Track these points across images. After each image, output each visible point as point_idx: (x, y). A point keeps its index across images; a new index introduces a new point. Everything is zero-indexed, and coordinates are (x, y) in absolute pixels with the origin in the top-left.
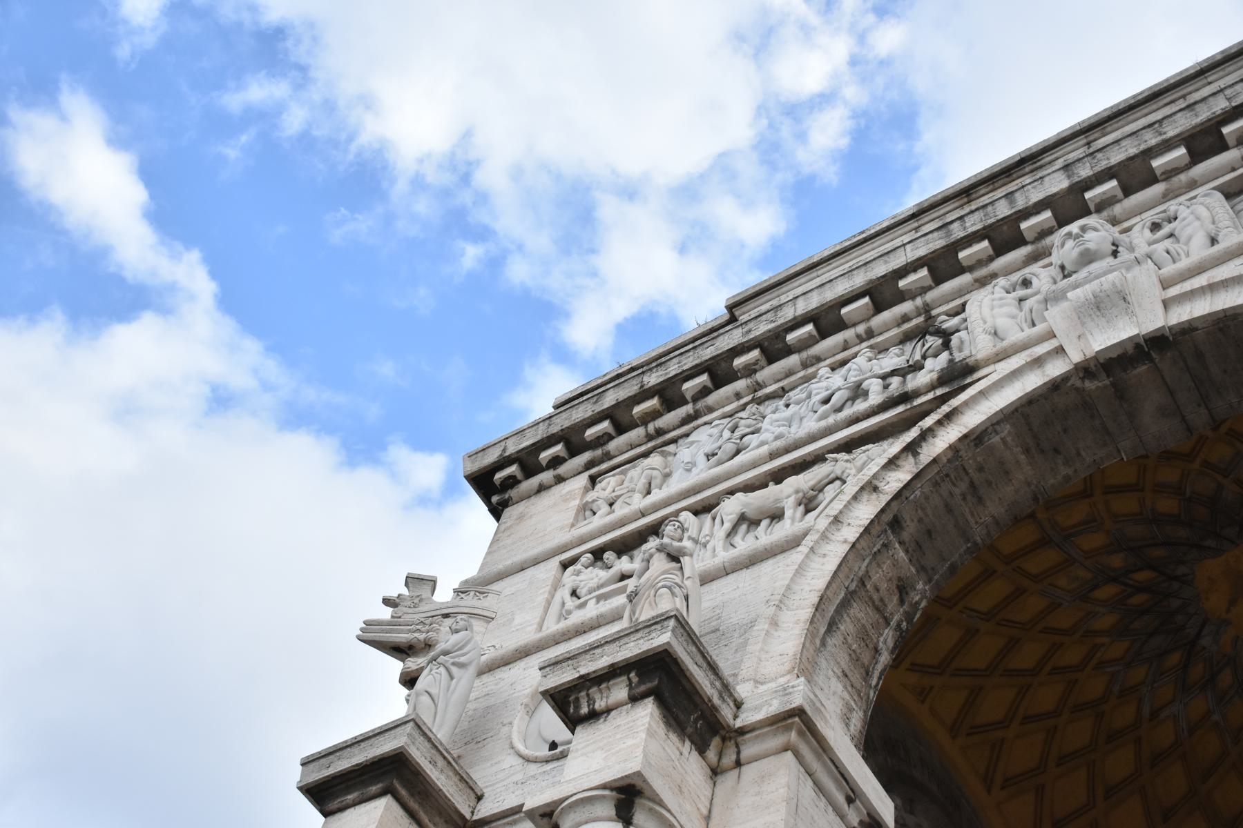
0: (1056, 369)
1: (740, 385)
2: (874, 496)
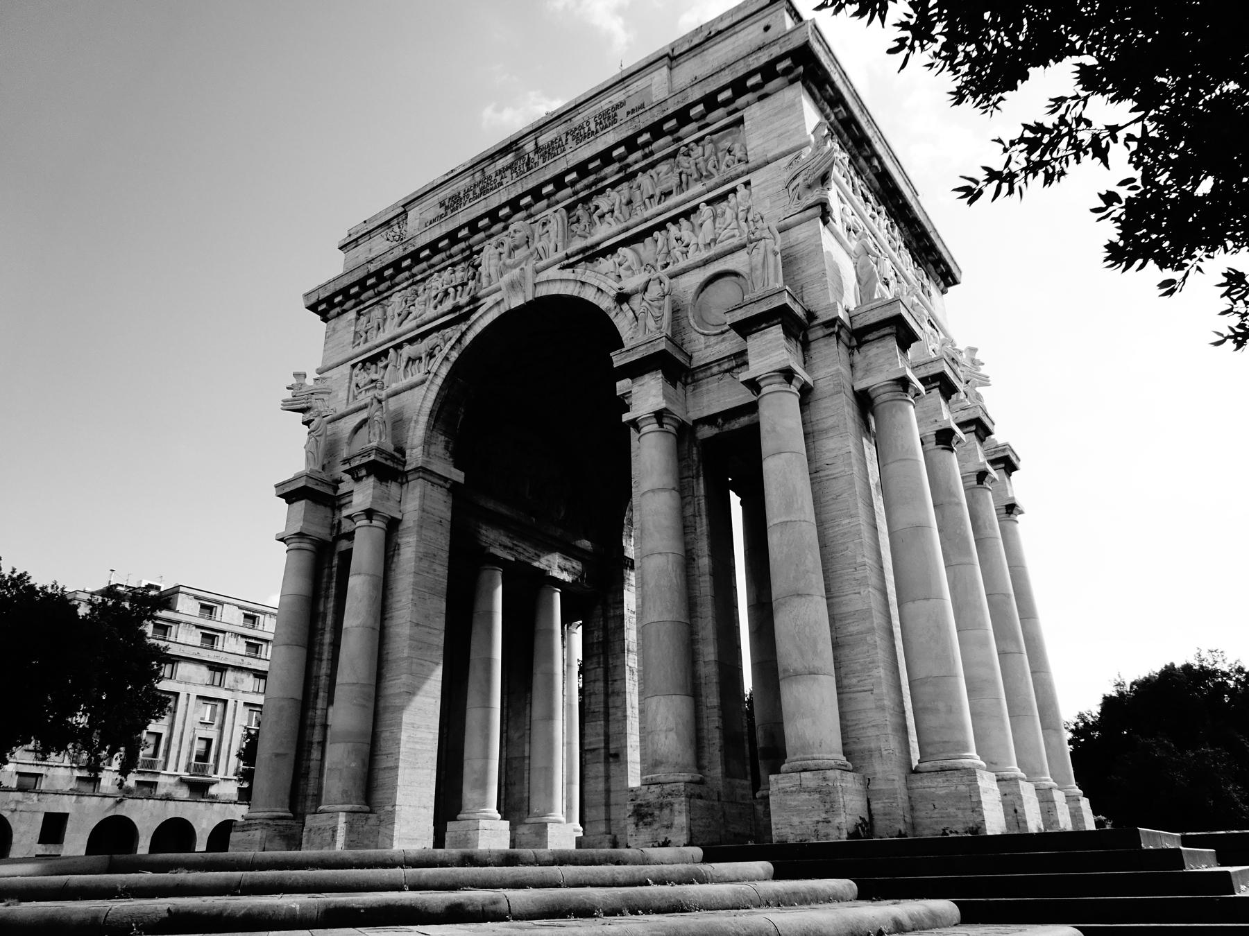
0: (503, 308)
1: (407, 274)
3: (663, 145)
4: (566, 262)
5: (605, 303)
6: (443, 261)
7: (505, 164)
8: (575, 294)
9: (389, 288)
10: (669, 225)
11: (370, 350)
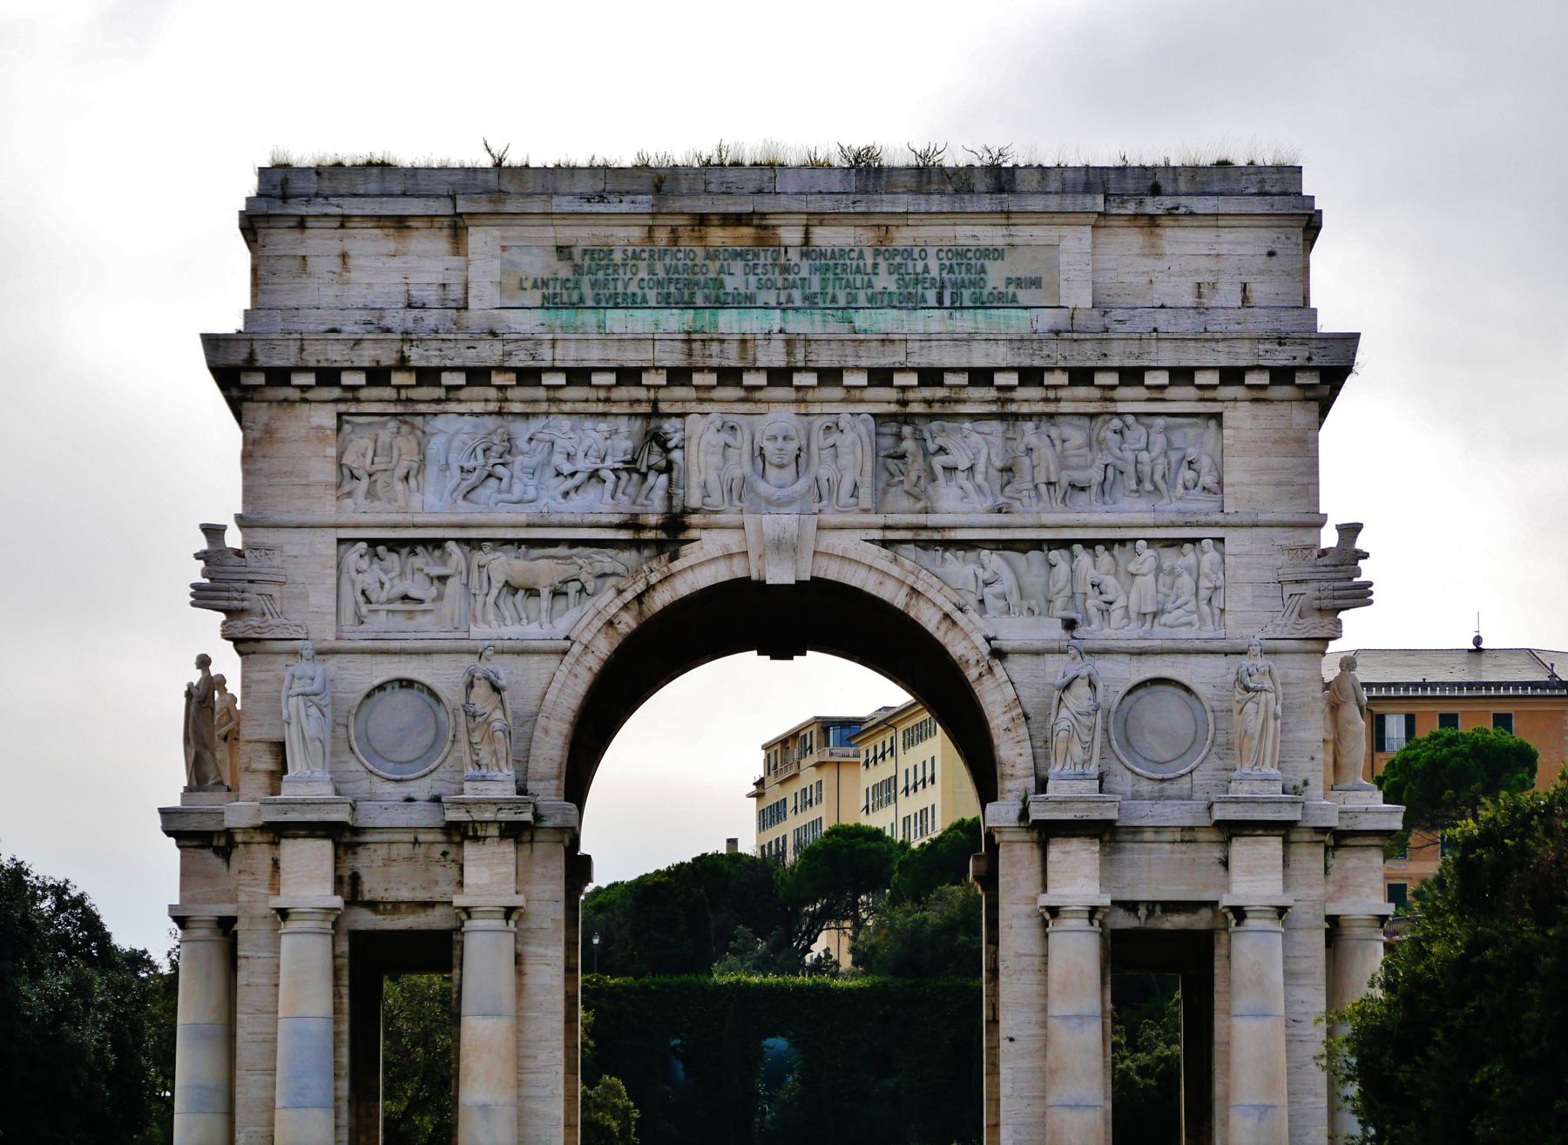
0: (738, 570)
1: (492, 393)
2: (610, 631)
3: (1080, 398)
4: (878, 535)
5: (963, 647)
6: (587, 401)
7: (729, 242)
8: (899, 600)
9: (438, 401)
10: (1077, 548)
11: (395, 526)
